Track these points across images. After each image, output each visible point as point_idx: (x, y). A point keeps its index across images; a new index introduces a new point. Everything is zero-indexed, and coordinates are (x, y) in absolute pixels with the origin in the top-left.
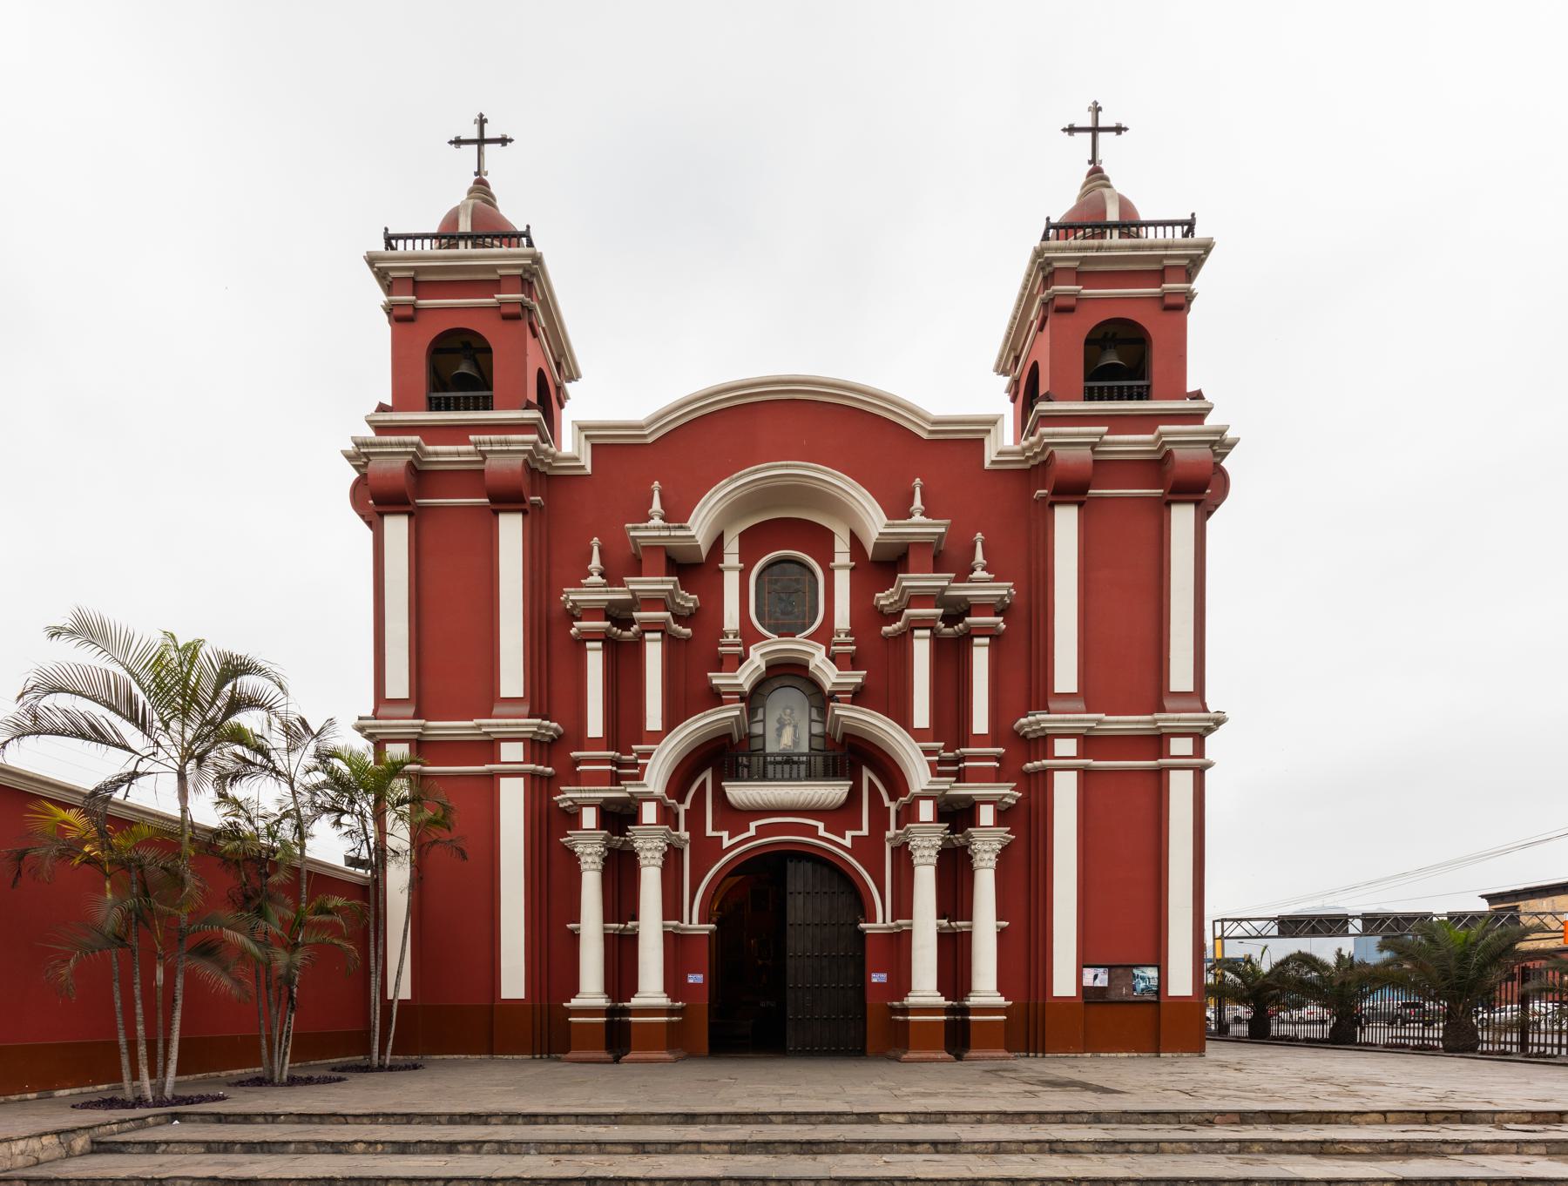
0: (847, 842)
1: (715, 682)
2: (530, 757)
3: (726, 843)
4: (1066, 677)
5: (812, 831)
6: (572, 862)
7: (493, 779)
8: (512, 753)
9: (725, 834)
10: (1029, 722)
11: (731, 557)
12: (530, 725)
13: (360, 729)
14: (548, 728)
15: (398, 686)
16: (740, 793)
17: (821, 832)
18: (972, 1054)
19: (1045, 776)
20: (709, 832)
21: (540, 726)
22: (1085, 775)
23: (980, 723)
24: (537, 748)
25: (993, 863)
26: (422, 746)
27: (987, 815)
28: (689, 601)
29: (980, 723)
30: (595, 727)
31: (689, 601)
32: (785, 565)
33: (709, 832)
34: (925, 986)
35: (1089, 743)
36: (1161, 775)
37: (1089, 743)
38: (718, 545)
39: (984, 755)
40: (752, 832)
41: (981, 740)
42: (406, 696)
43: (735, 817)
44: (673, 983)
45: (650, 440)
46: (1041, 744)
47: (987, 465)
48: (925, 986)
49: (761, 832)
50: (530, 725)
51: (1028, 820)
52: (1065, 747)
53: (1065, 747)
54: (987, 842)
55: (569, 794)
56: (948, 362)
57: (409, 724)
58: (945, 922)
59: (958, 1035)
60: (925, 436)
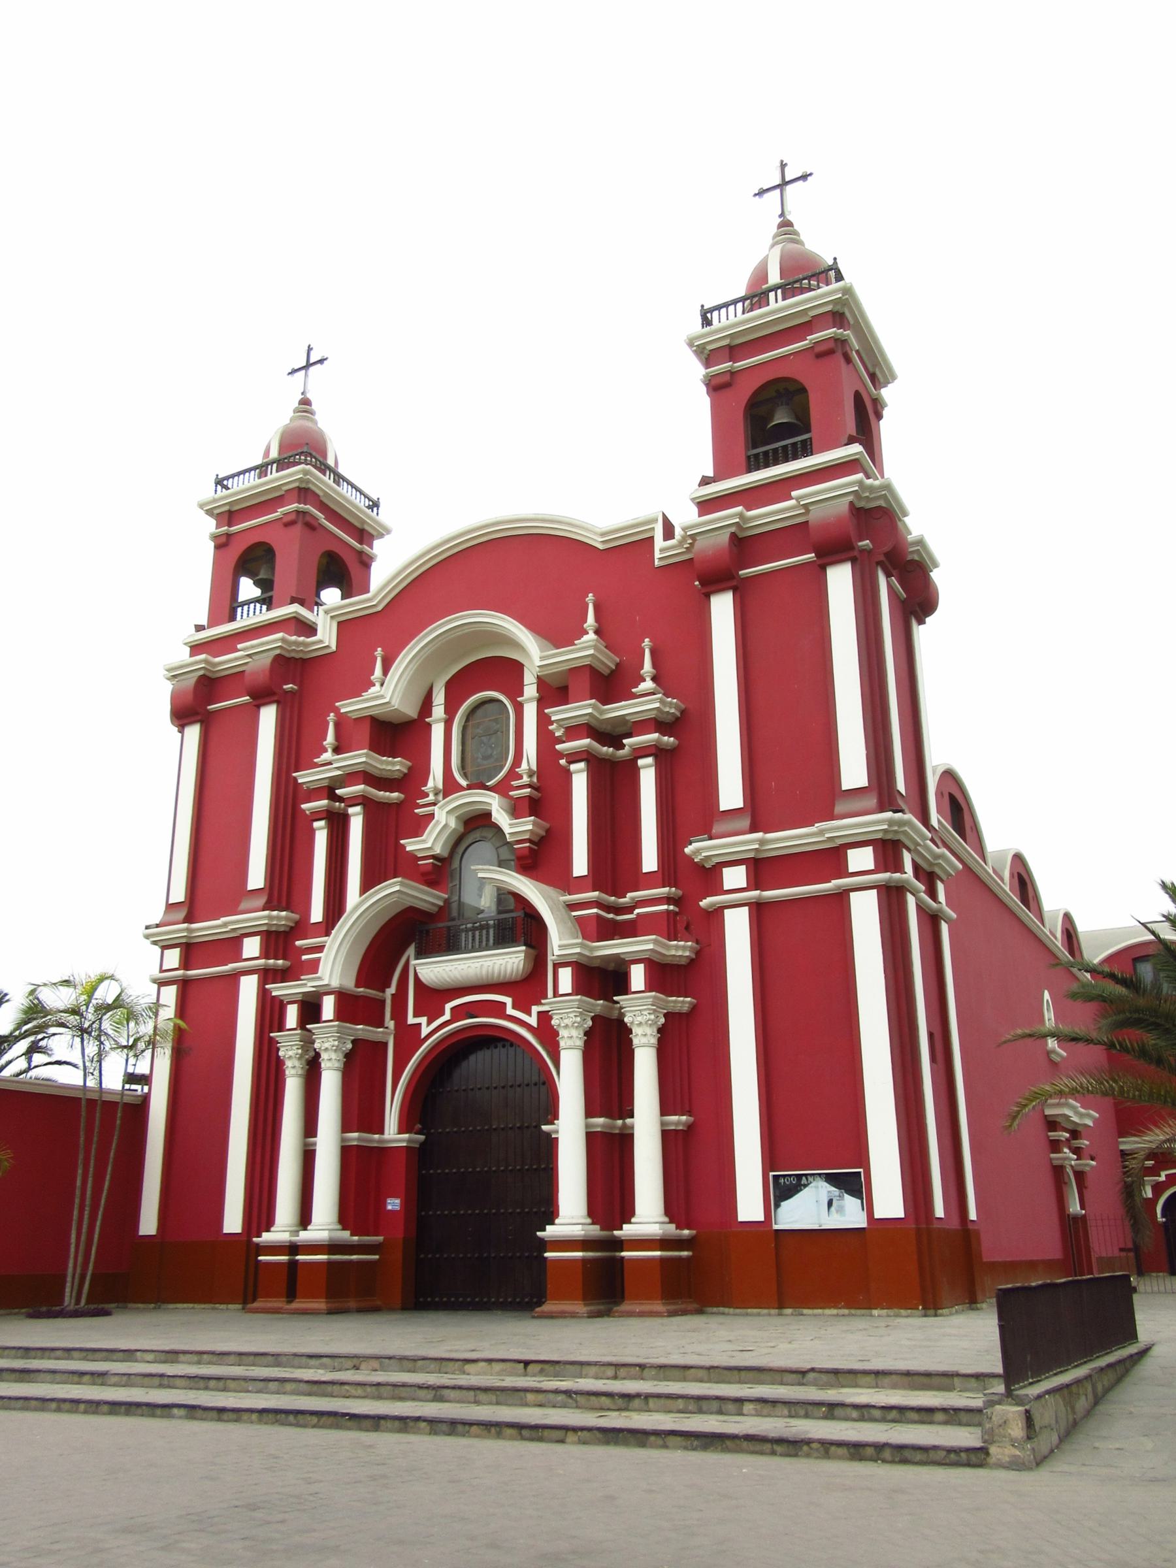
0: (533, 1021)
1: (408, 849)
2: (266, 953)
3: (425, 1031)
4: (731, 792)
5: (498, 1009)
6: (280, 1063)
7: (235, 977)
8: (252, 947)
9: (423, 1020)
10: (699, 849)
11: (438, 711)
12: (261, 918)
13: (147, 937)
14: (278, 918)
15: (179, 894)
16: (435, 970)
17: (510, 1011)
18: (625, 1307)
19: (716, 916)
20: (411, 1020)
21: (270, 918)
22: (759, 911)
23: (650, 862)
24: (277, 942)
25: (654, 1041)
26: (191, 952)
27: (638, 976)
28: (395, 765)
29: (650, 862)
30: (317, 914)
31: (395, 765)
32: (480, 712)
33: (411, 1020)
34: (572, 1215)
35: (761, 870)
36: (841, 899)
37: (761, 870)
38: (426, 706)
39: (650, 900)
40: (447, 1016)
41: (650, 880)
42: (741, 805)
43: (432, 998)
44: (351, 1210)
45: (380, 608)
46: (710, 877)
47: (657, 563)
48: (572, 1215)
49: (458, 1013)
50: (261, 918)
51: (692, 980)
52: (735, 877)
53: (735, 877)
54: (642, 1014)
55: (278, 990)
56: (643, 464)
57: (179, 930)
58: (599, 1121)
59: (607, 1281)
60: (601, 547)
